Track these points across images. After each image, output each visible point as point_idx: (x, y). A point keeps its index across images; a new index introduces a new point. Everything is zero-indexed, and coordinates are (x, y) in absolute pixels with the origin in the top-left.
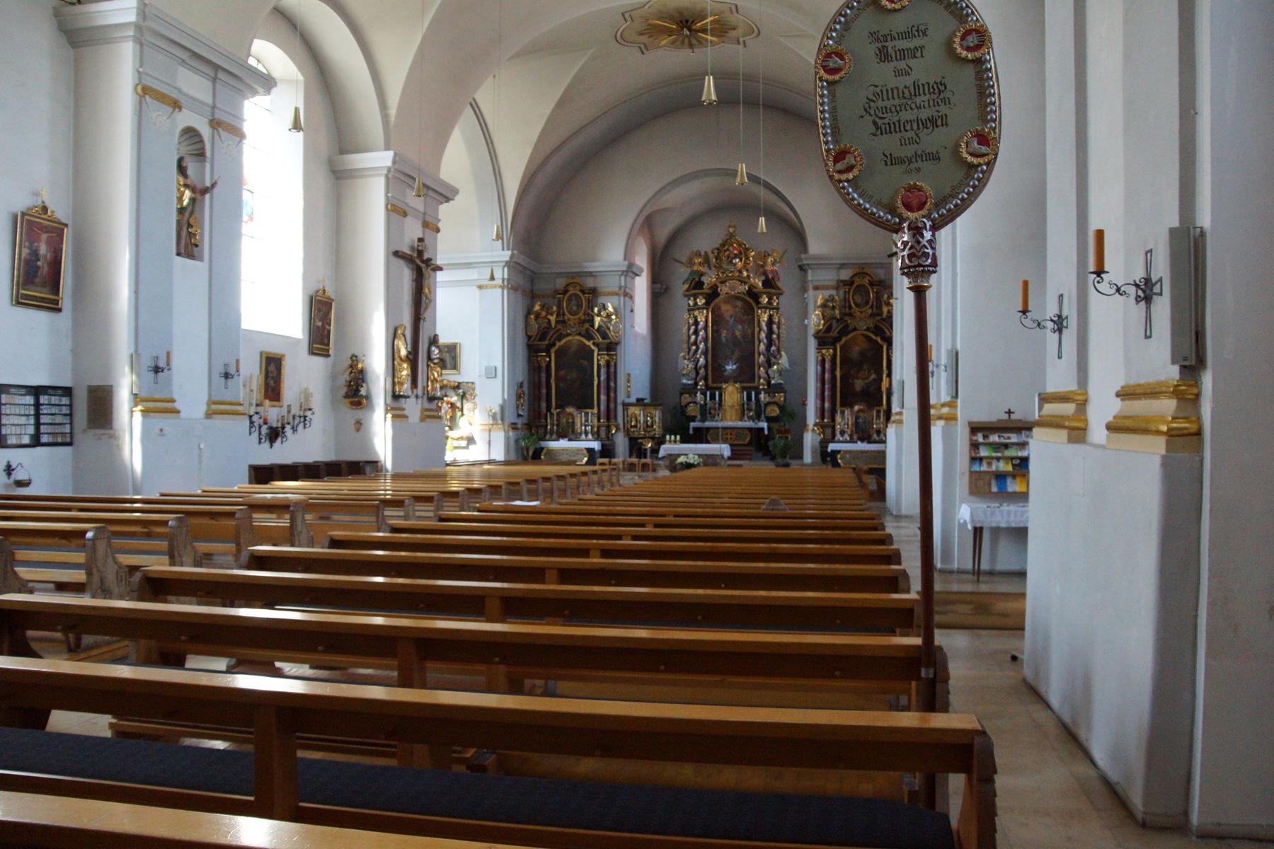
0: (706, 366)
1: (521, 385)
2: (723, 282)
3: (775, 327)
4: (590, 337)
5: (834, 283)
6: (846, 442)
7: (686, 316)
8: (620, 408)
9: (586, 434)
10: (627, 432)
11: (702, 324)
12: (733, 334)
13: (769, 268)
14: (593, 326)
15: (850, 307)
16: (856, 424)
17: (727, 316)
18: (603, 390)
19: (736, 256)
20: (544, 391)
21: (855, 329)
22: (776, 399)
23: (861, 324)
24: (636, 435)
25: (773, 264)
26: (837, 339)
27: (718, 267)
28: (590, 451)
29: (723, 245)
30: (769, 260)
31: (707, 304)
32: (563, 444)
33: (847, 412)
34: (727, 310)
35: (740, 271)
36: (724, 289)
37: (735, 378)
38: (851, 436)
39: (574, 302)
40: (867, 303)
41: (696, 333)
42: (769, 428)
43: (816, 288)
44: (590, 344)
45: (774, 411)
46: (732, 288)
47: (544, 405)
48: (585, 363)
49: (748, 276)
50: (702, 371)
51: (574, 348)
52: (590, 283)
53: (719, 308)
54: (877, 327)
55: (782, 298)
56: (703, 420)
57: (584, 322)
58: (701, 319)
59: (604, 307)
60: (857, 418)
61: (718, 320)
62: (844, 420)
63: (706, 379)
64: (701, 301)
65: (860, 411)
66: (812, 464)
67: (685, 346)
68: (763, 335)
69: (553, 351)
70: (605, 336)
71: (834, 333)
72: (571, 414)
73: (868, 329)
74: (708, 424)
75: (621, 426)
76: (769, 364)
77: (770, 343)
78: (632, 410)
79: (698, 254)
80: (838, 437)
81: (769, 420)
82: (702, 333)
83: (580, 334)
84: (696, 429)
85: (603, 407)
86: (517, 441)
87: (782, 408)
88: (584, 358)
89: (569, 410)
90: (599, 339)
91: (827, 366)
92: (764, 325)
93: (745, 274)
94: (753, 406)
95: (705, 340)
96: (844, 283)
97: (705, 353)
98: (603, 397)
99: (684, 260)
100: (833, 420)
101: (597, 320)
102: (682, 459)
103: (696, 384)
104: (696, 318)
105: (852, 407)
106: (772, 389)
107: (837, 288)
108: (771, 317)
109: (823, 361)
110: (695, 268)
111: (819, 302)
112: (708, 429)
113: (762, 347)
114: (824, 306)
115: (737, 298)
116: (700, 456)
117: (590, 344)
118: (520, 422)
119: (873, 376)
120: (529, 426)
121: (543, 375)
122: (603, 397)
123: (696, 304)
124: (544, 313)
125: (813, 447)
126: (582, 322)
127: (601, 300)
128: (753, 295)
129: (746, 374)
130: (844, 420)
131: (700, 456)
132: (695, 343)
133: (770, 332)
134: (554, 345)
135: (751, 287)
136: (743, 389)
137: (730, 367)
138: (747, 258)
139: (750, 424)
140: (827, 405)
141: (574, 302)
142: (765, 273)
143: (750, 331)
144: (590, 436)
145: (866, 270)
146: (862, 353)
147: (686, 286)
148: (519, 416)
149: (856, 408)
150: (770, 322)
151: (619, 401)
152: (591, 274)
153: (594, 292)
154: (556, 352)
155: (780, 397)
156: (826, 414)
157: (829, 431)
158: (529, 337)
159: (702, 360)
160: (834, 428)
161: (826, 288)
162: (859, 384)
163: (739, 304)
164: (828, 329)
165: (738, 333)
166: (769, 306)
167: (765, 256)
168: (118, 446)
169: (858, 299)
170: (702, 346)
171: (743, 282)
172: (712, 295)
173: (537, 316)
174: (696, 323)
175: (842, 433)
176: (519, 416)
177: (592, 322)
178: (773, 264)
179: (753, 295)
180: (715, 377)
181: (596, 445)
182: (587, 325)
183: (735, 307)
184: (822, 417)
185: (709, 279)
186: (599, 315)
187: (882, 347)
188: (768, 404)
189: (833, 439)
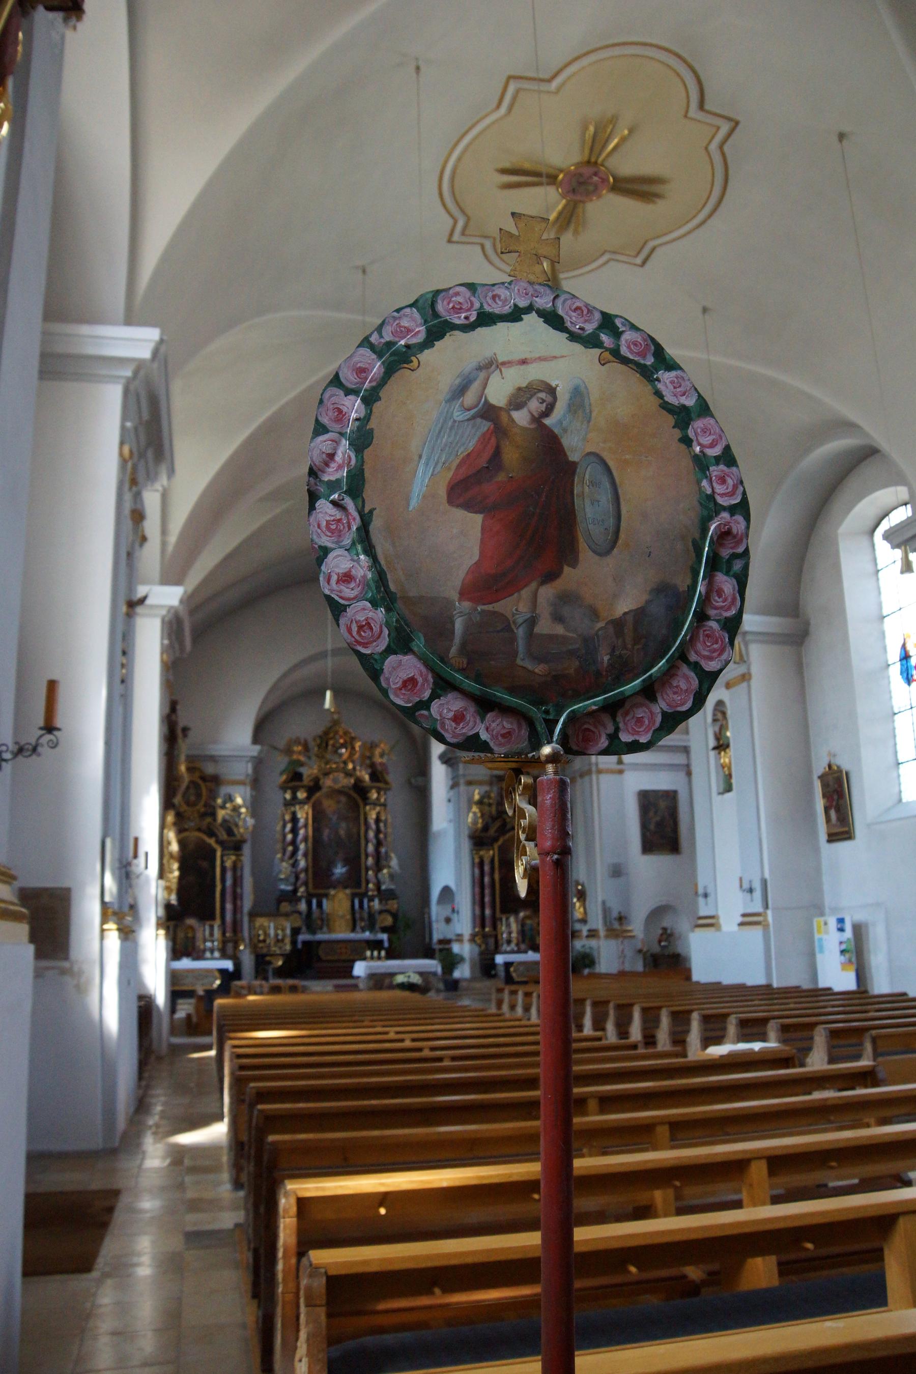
0: (306, 870)
2: (326, 774)
3: (382, 825)
4: (211, 833)
5: (486, 778)
6: (512, 952)
7: (280, 809)
8: (246, 919)
11: (302, 822)
13: (378, 760)
14: (215, 820)
16: (522, 932)
18: (229, 897)
19: (343, 746)
22: (388, 907)
24: (265, 951)
25: (382, 755)
26: (496, 840)
27: (320, 757)
28: (223, 972)
29: (326, 733)
30: (377, 752)
31: (308, 798)
33: (512, 919)
34: (329, 805)
35: (345, 763)
36: (327, 782)
37: (343, 883)
38: (517, 945)
39: (192, 791)
41: (294, 831)
42: (390, 940)
43: (469, 783)
44: (212, 841)
45: (389, 921)
46: (335, 781)
48: (205, 864)
49: (354, 768)
50: (302, 876)
52: (210, 769)
55: (388, 793)
56: (314, 932)
57: (203, 815)
58: (301, 815)
59: (230, 798)
60: (523, 925)
61: (318, 816)
62: (511, 927)
63: (306, 884)
64: (301, 795)
65: (525, 917)
66: (473, 979)
67: (279, 846)
68: (371, 834)
70: (230, 832)
71: (492, 832)
74: (320, 936)
75: (247, 941)
76: (378, 868)
77: (379, 844)
78: (260, 921)
79: (297, 742)
80: (505, 947)
81: (384, 930)
82: (302, 832)
83: (199, 830)
84: (305, 943)
85: (229, 917)
87: (395, 916)
89: (191, 921)
90: (223, 836)
91: (487, 868)
92: (372, 822)
93: (350, 766)
94: (366, 916)
95: (305, 839)
96: (500, 779)
97: (305, 855)
98: (229, 906)
99: (282, 744)
100: (495, 927)
101: (221, 814)
102: (400, 979)
103: (295, 891)
104: (294, 815)
105: (516, 913)
106: (385, 896)
107: (491, 784)
108: (378, 814)
109: (481, 864)
110: (295, 757)
111: (477, 797)
112: (319, 943)
113: (371, 848)
114: (480, 803)
115: (340, 792)
116: (421, 974)
117: (212, 841)
122: (229, 906)
123: (294, 797)
125: (471, 960)
126: (203, 815)
127: (224, 790)
128: (360, 790)
129: (354, 880)
130: (511, 927)
131: (421, 974)
132: (293, 843)
133: (378, 831)
135: (359, 781)
136: (354, 895)
137: (339, 870)
138: (353, 748)
139: (367, 935)
140: (488, 912)
141: (192, 791)
142: (372, 766)
143: (355, 830)
144: (217, 954)
147: (284, 777)
149: (522, 914)
150: (378, 820)
152: (213, 759)
153: (216, 780)
155: (393, 905)
156: (488, 922)
157: (491, 941)
160: (496, 937)
161: (480, 783)
163: (343, 799)
164: (486, 828)
165: (342, 832)
166: (375, 804)
167: (373, 746)
168: (78, 987)
170: (302, 846)
171: (348, 774)
172: (314, 788)
174: (294, 820)
175: (509, 942)
177: (214, 815)
178: (382, 755)
179: (360, 790)
180: (320, 879)
181: (228, 965)
182: (209, 820)
183: (338, 802)
184: (483, 926)
185: (309, 771)
186: (223, 807)
188: (381, 912)
189: (497, 950)
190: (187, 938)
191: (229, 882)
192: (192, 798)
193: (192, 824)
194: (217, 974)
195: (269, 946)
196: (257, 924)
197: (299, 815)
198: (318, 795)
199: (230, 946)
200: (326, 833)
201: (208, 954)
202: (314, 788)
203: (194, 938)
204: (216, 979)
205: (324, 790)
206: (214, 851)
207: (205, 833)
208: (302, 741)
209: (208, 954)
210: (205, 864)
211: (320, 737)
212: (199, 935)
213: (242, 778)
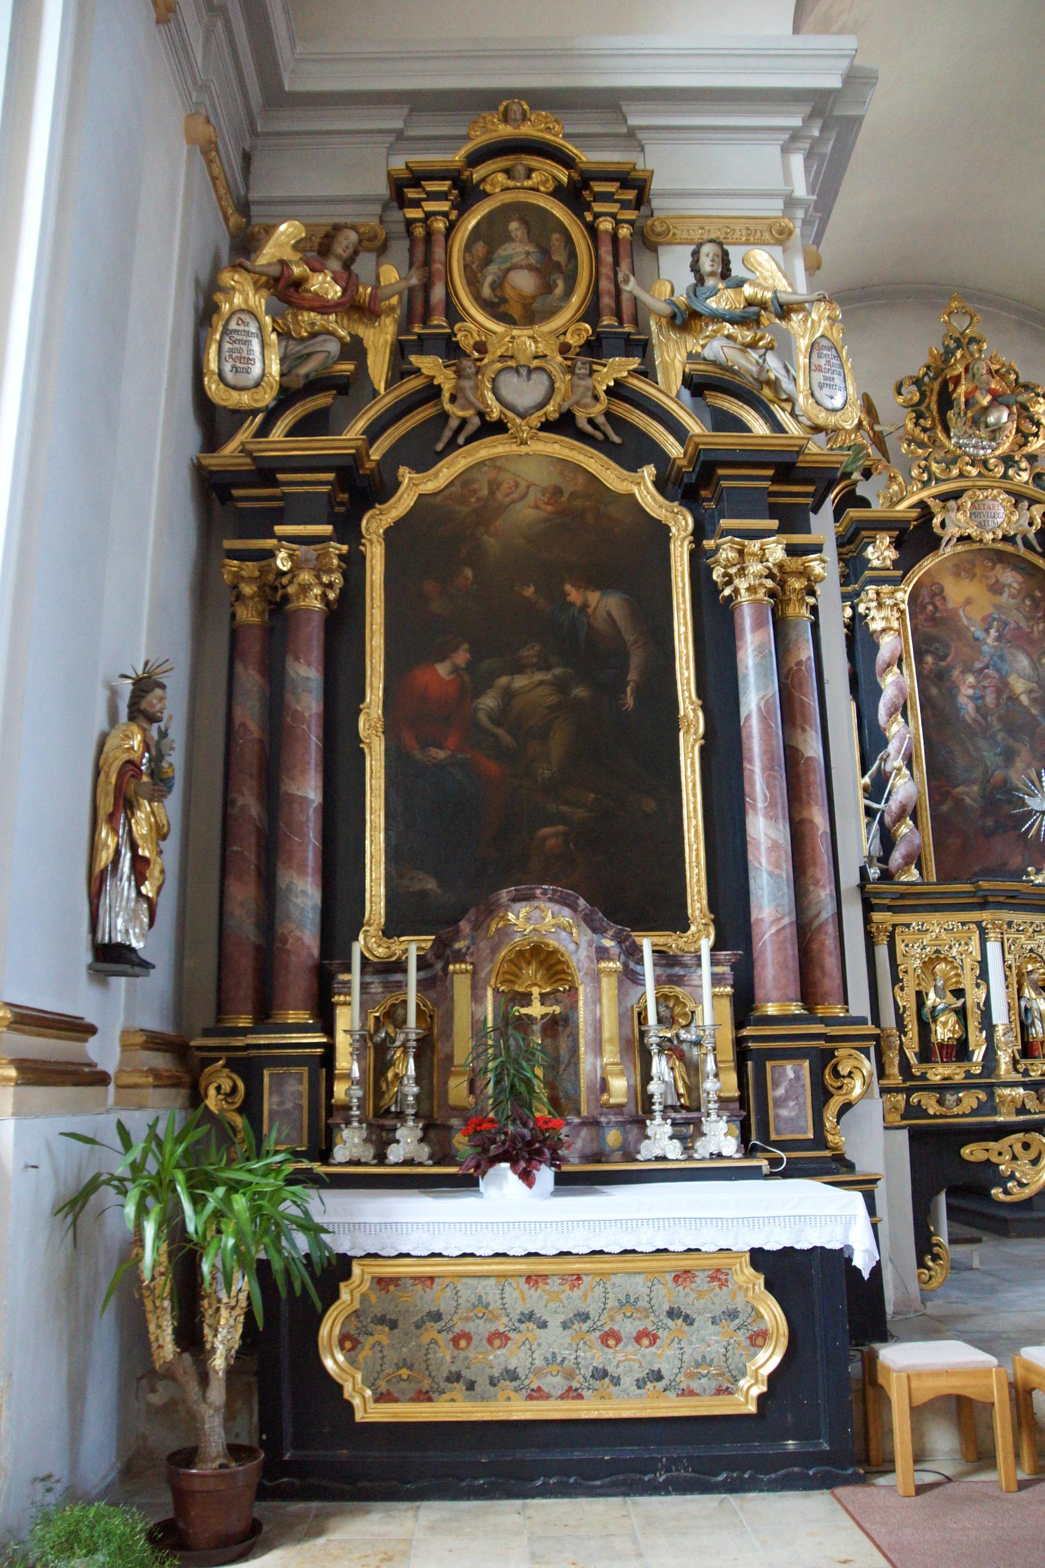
1: (141, 698)
9: (688, 1126)
12: (1002, 686)
17: (971, 619)
19: (997, 399)
20: (310, 789)
32: (509, 1214)
34: (969, 600)
36: (955, 522)
39: (518, 248)
47: (304, 894)
48: (605, 605)
51: (526, 513)
53: (939, 593)
57: (595, 348)
69: (376, 523)
72: (549, 962)
83: (563, 424)
86: (76, 1205)
88: (599, 578)
89: (540, 919)
98: (765, 832)
115: (999, 557)
118: (120, 1015)
120: (181, 1058)
121: (306, 674)
148: (111, 958)
154: (392, 536)
158: (213, 421)
163: (1010, 577)
165: (1019, 686)
172: (916, 538)
173: (286, 290)
176: (111, 958)
182: (618, 368)
183: (996, 589)
190: (512, 1024)
191: (756, 695)
192: (524, 282)
193: (523, 392)
194: (752, 1282)
195: (987, 1081)
196: (913, 954)
197: (876, 626)
198: (928, 563)
199: (790, 1078)
200: (967, 687)
201: (661, 1141)
202: (916, 538)
203: (559, 1026)
204: (759, 1339)
205: (947, 551)
206: (661, 532)
207: (604, 446)
209: (661, 1141)
210: (605, 605)
211: (918, 382)
212: (598, 1009)
213: (774, 207)
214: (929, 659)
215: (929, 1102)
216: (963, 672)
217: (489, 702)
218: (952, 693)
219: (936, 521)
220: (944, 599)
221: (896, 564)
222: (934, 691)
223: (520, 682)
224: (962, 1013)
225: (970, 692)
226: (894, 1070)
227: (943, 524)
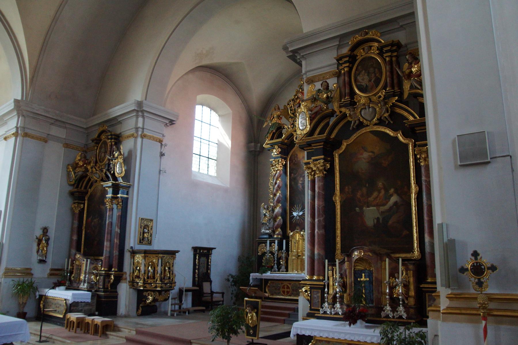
10: (133, 284)
15: (352, 94)
21: (361, 125)
23: (366, 114)
40: (377, 81)
54: (393, 115)
60: (357, 274)
65: (360, 260)
69: (86, 198)
73: (381, 122)
114: (314, 99)
119: (394, 199)
124: (81, 163)
134: (87, 193)
141: (103, 150)
145: (370, 36)
146: (375, 162)
151: (127, 247)
159: (278, 210)
162: (371, 215)
169: (364, 79)
187: (406, 146)
208: (282, 107)
214: (292, 175)
215: (147, 286)
216: (301, 177)
217: (93, 223)
218: (297, 183)
219: (295, 137)
220: (297, 158)
221: (280, 153)
222: (293, 183)
223: (95, 220)
224: (139, 270)
225: (301, 182)
226: (131, 279)
227: (296, 138)
